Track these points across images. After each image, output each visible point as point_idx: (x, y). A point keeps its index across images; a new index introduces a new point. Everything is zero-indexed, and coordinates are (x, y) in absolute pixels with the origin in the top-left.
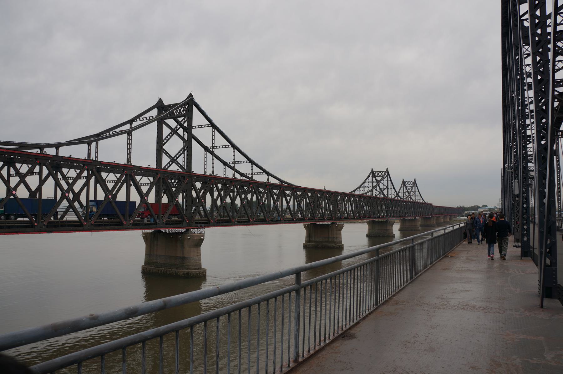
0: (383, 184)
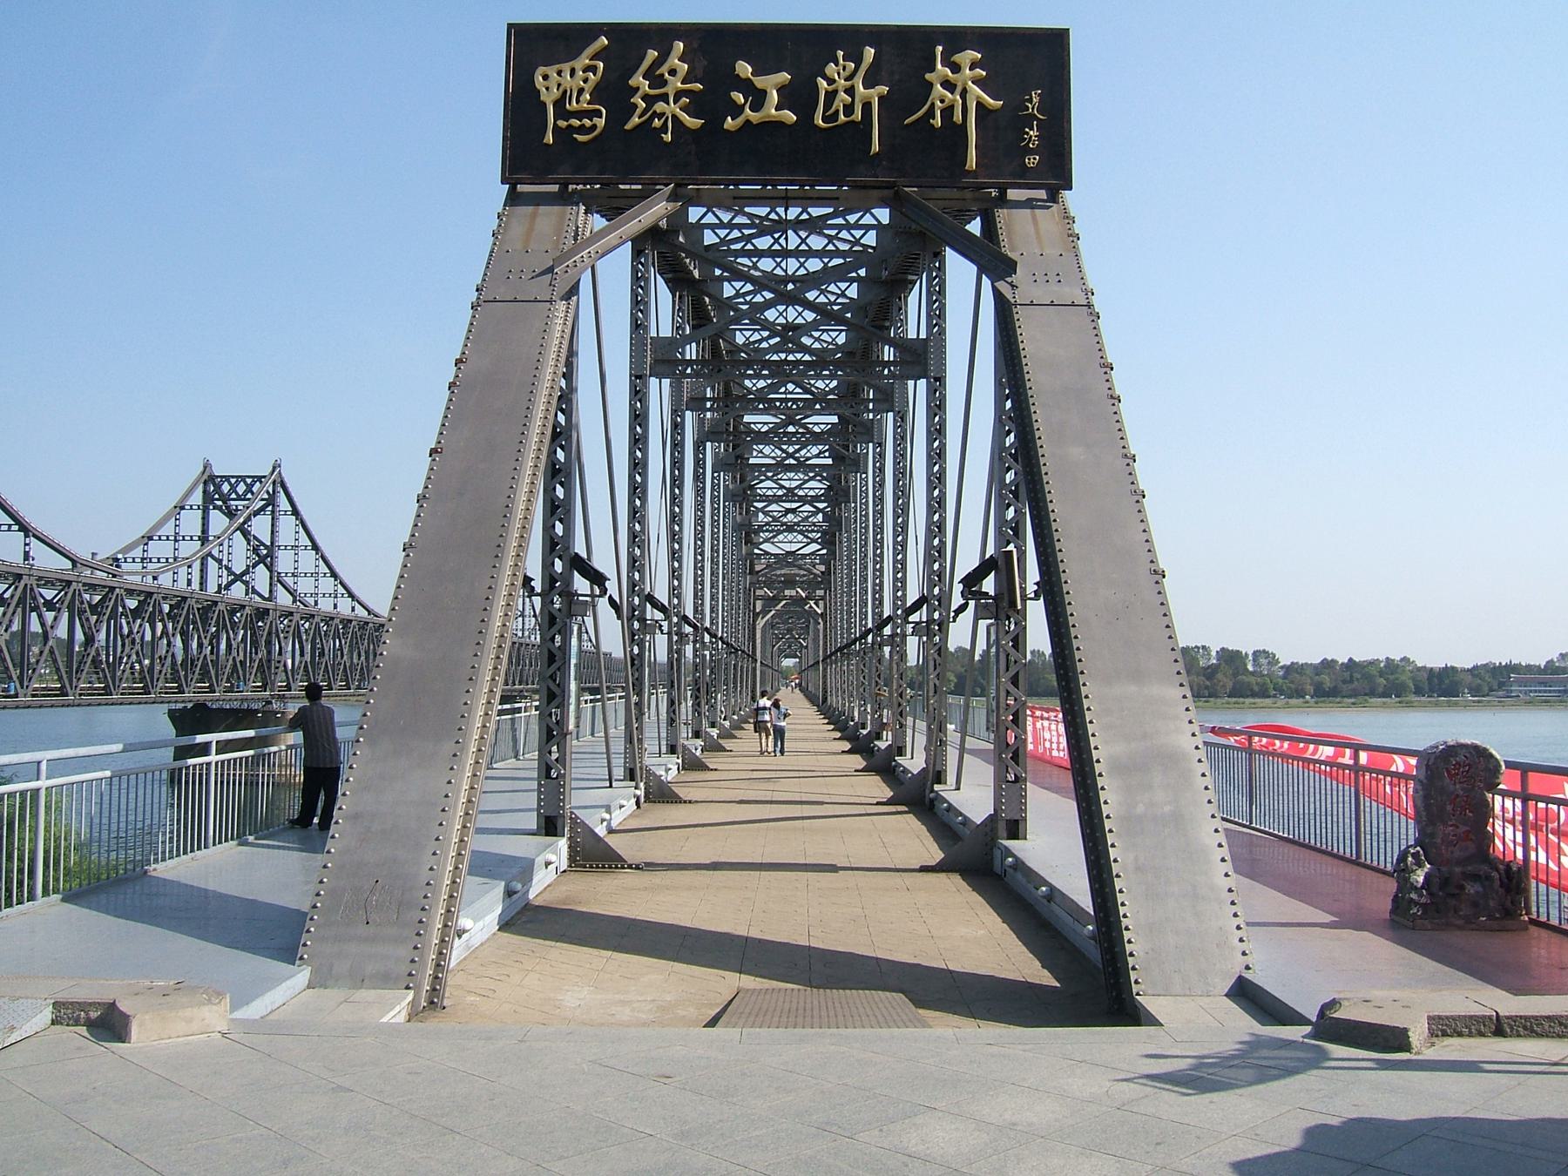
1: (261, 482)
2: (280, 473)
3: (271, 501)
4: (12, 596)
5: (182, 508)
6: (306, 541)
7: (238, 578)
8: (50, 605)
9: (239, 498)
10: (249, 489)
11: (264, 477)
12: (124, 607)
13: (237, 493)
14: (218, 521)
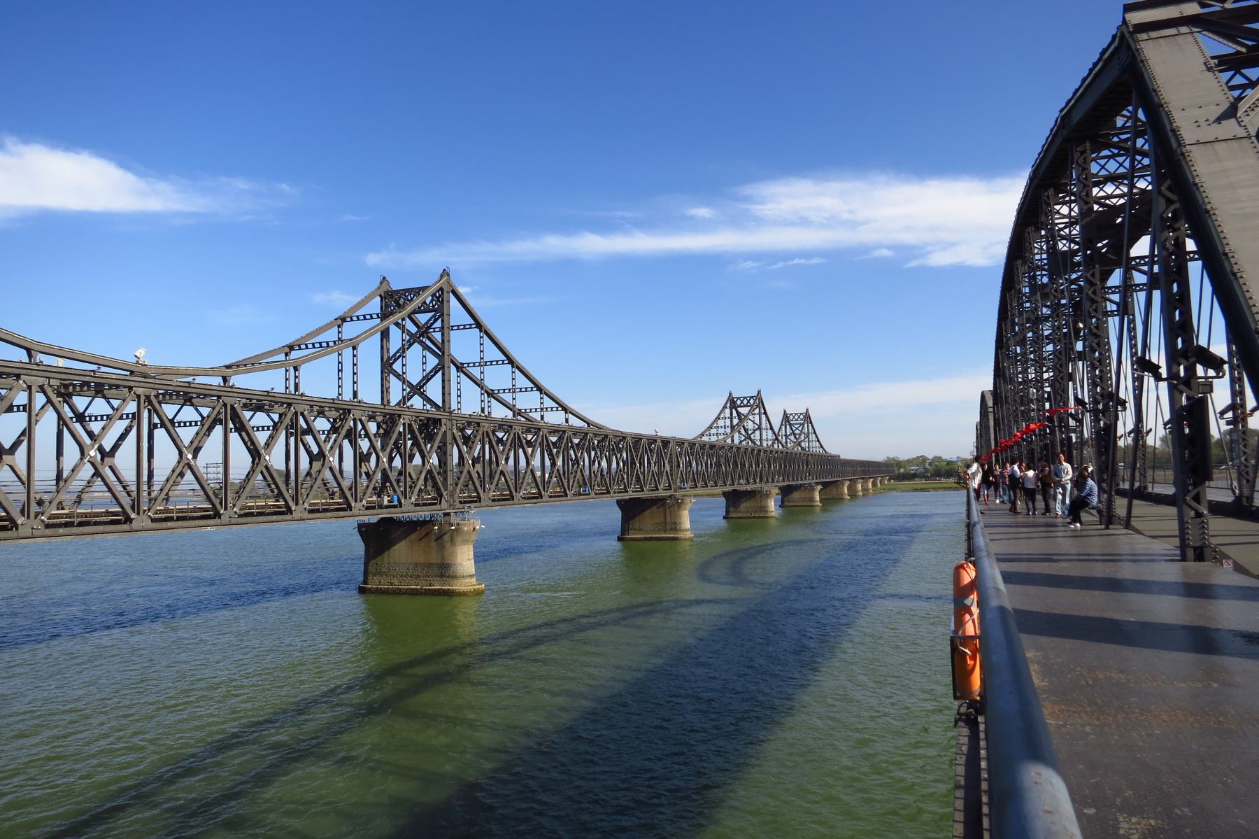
0: (753, 422)
4: (507, 439)
8: (529, 443)
12: (571, 442)
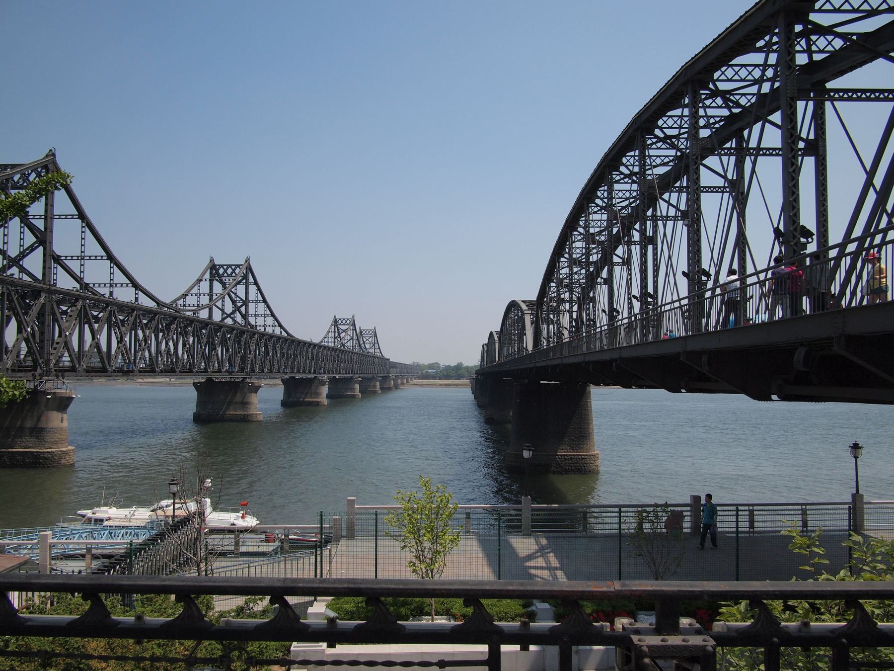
1: (240, 268)
2: (249, 264)
3: (245, 277)
5: (201, 280)
6: (260, 298)
7: (229, 316)
9: (228, 276)
10: (234, 271)
11: (242, 265)
13: (227, 273)
14: (218, 288)
